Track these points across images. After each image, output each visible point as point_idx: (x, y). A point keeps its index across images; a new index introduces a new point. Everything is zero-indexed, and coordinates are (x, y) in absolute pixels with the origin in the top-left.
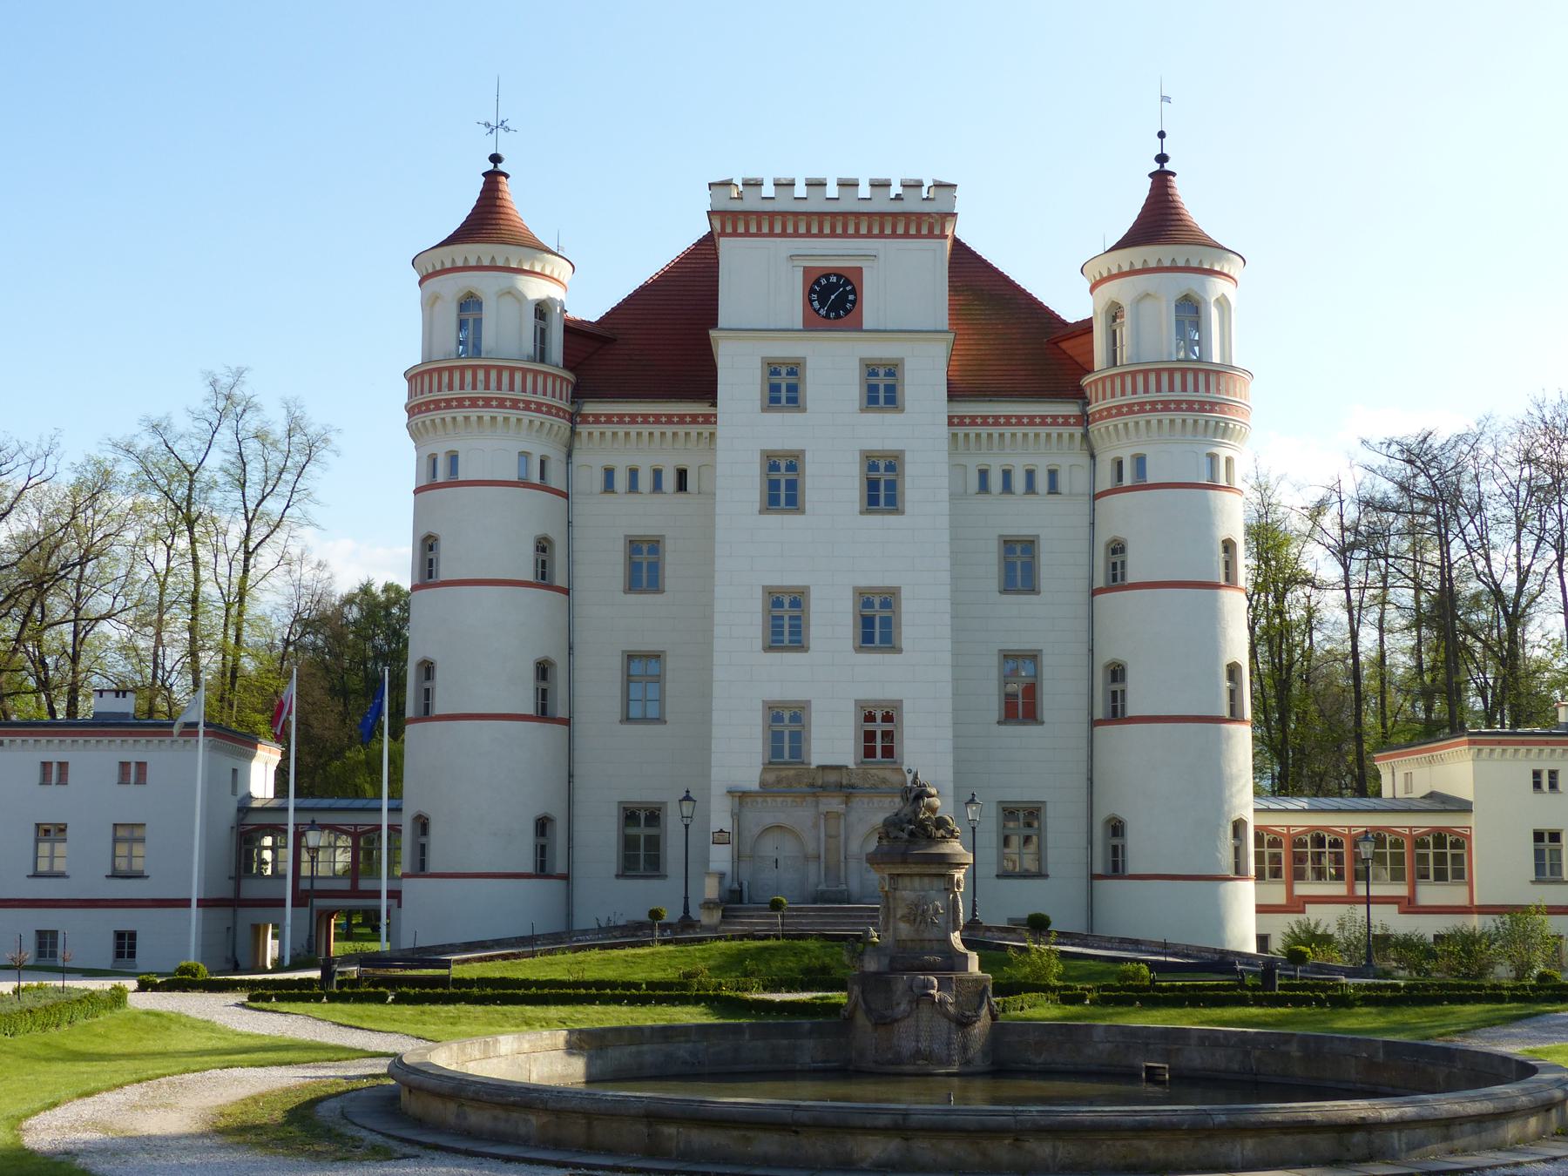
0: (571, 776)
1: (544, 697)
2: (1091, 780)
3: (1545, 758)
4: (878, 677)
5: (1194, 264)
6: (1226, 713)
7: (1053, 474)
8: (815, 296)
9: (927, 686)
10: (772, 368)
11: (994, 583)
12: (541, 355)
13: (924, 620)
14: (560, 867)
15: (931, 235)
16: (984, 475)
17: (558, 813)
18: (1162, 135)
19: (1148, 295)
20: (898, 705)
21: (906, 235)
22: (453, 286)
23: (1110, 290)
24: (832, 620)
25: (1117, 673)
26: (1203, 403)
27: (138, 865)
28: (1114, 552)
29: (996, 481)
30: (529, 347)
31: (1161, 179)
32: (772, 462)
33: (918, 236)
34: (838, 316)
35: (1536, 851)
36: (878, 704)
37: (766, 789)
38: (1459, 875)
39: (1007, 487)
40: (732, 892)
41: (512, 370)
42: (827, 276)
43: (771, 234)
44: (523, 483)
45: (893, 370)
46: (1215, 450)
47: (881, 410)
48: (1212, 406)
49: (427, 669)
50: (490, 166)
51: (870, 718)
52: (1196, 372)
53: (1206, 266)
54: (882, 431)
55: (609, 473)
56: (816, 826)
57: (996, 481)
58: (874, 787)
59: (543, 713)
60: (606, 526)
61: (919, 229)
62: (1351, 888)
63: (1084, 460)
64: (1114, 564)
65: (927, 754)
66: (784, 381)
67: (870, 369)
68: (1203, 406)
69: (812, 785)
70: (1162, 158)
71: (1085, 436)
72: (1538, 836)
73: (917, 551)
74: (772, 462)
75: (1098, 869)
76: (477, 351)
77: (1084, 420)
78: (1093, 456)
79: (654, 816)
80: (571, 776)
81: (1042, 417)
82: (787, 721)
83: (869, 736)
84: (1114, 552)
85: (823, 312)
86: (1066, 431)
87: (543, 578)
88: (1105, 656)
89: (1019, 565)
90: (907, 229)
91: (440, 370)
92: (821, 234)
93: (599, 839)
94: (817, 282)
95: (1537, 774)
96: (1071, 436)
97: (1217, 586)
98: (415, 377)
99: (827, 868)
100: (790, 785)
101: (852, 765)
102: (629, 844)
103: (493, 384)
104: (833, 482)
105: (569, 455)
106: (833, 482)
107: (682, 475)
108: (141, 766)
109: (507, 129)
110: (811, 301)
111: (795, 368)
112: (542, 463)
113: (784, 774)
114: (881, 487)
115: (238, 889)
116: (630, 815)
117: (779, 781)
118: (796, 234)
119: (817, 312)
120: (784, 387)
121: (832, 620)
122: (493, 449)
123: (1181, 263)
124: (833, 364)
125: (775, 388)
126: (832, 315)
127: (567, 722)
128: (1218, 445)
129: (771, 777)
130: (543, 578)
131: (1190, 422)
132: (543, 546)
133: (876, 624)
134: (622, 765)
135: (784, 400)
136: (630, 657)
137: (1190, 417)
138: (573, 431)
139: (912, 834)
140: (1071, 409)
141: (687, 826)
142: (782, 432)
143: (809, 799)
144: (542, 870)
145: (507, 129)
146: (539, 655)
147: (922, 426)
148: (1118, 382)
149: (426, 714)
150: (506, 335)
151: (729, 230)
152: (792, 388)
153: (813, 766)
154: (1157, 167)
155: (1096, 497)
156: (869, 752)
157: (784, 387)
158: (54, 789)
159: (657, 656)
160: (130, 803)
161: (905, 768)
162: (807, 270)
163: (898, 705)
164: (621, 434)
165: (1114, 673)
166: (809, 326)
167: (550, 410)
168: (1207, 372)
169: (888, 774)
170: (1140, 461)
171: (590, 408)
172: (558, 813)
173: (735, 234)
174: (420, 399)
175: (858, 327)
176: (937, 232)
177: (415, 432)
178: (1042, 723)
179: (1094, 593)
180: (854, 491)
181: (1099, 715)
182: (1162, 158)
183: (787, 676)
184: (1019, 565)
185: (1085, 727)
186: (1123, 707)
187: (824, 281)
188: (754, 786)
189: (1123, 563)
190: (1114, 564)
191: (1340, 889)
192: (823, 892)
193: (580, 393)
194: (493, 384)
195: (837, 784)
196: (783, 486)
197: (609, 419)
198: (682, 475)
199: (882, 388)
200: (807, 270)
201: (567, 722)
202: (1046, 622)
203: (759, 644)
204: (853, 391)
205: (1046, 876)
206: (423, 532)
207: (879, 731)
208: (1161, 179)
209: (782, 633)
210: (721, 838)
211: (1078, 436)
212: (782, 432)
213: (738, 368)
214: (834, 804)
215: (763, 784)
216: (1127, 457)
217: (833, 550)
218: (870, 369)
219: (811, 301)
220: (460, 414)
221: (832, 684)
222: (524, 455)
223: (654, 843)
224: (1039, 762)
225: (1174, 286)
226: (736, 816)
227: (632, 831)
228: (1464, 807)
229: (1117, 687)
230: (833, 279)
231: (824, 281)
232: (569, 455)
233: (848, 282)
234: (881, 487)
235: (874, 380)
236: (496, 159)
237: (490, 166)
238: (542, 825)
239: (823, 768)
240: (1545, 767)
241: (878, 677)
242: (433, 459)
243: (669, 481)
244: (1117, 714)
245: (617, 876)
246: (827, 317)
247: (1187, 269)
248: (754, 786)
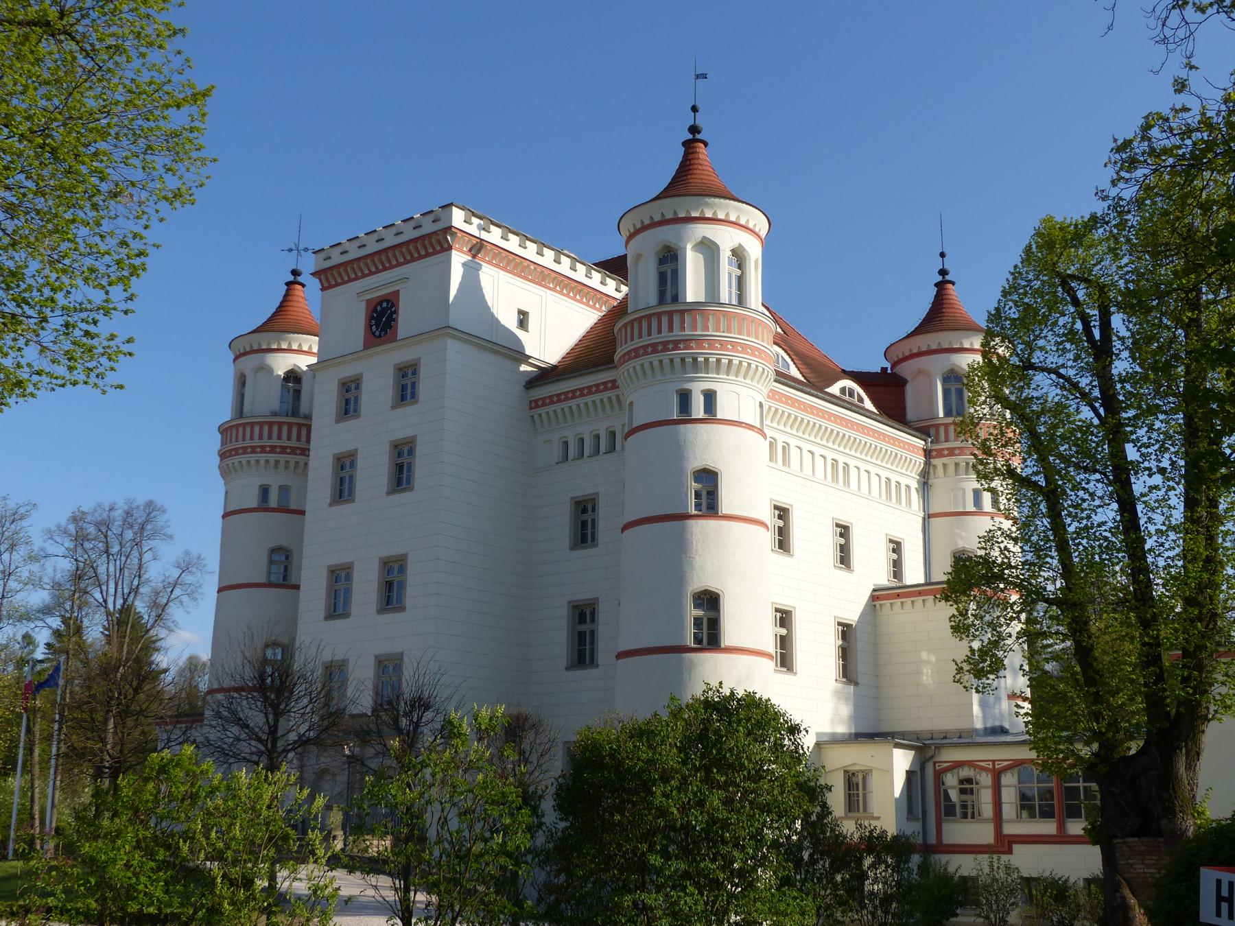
5: (669, 216)
6: (690, 642)
11: (566, 542)
18: (694, 109)
26: (665, 344)
42: (380, 303)
44: (263, 507)
46: (687, 386)
48: (687, 342)
52: (670, 314)
53: (682, 215)
54: (404, 422)
62: (1061, 826)
68: (665, 346)
70: (694, 129)
94: (375, 310)
97: (689, 517)
106: (373, 471)
110: (371, 326)
119: (374, 334)
123: (657, 218)
128: (692, 380)
131: (656, 363)
137: (655, 358)
162: (368, 302)
166: (367, 346)
168: (683, 312)
176: (446, 246)
182: (694, 129)
187: (379, 308)
191: (1048, 827)
199: (406, 388)
200: (368, 302)
219: (371, 326)
222: (265, 491)
230: (385, 305)
231: (379, 308)
236: (295, 273)
247: (665, 222)
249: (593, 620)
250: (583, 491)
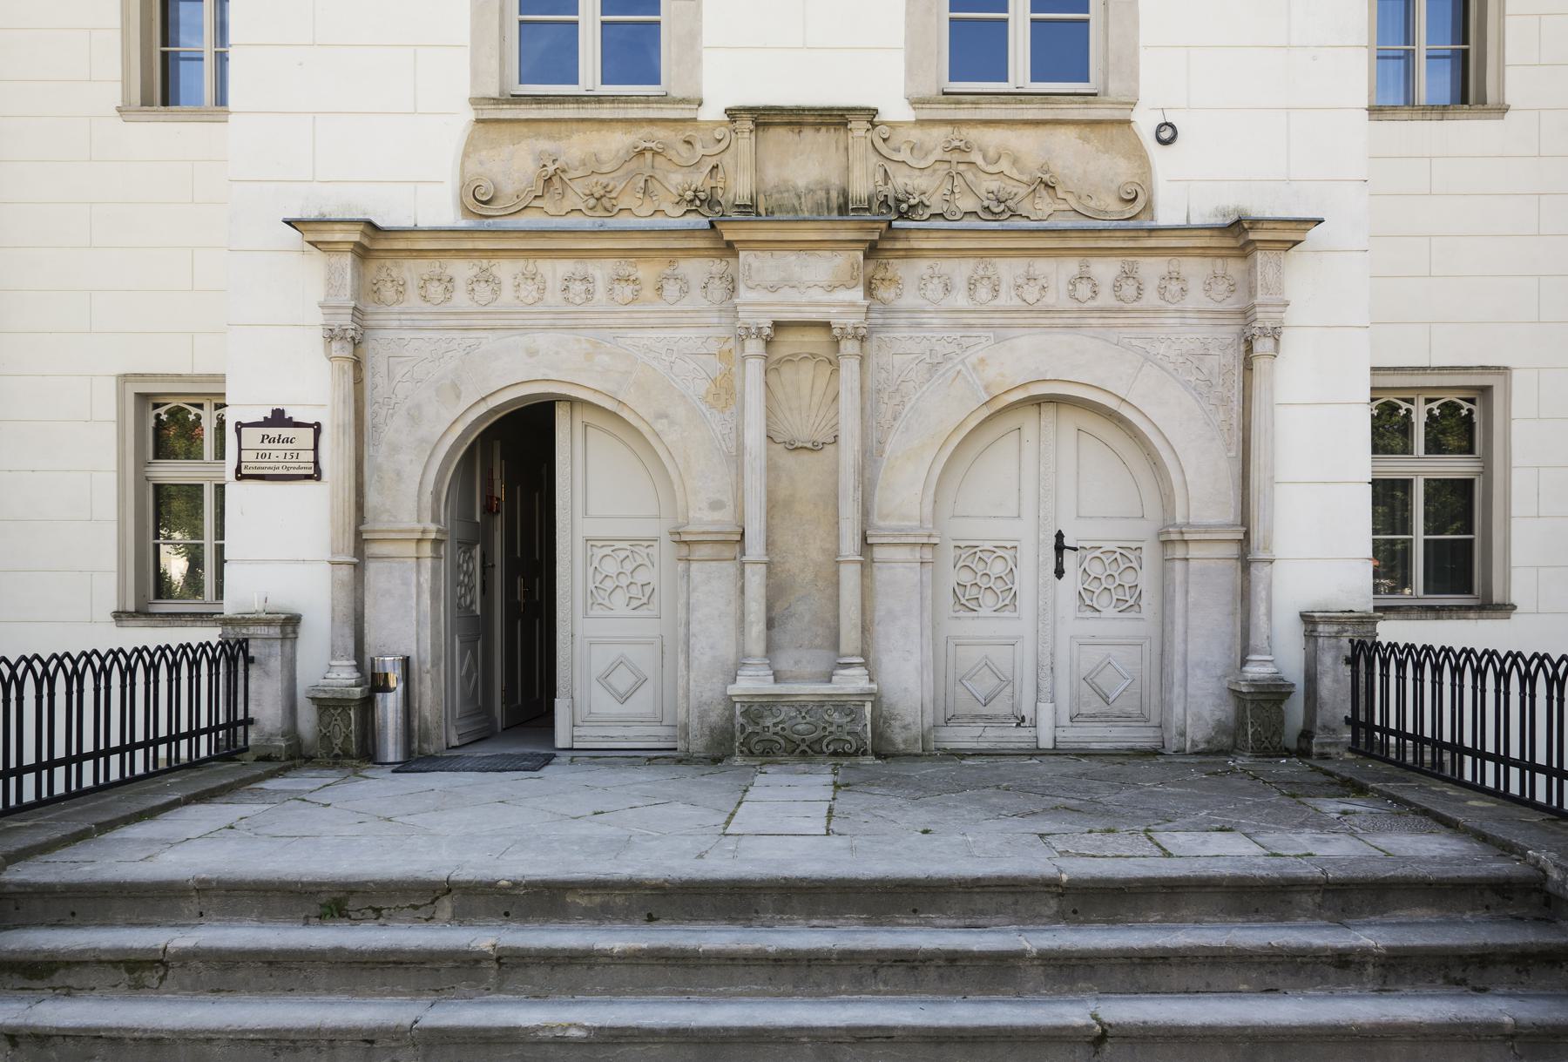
37: (488, 227)
40: (327, 705)
56: (726, 393)
58: (999, 209)
69: (702, 201)
99: (775, 592)
100: (602, 201)
101: (894, 109)
113: (575, 148)
117: (551, 180)
129: (514, 164)
143: (696, 269)
153: (712, 111)
161: (1145, 123)
169: (1067, 153)
178: (1502, 110)
188: (439, 208)
192: (756, 708)
214: (816, 282)
215: (478, 200)
226: (354, 345)
239: (764, 118)
248: (439, 208)
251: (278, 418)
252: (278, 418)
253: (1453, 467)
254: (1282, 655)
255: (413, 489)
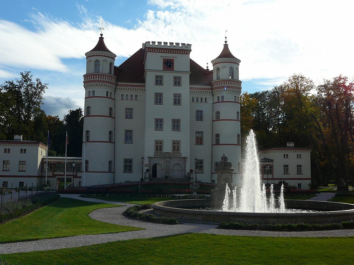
0: (115, 153)
1: (110, 138)
2: (212, 155)
3: (286, 152)
4: (177, 136)
7: (206, 99)
8: (165, 64)
9: (185, 137)
10: (157, 77)
12: (110, 73)
13: (185, 125)
14: (113, 171)
15: (187, 54)
16: (193, 98)
17: (113, 160)
18: (226, 38)
19: (224, 67)
20: (180, 141)
21: (182, 53)
22: (94, 59)
23: (218, 65)
24: (168, 125)
25: (218, 136)
27: (24, 169)
28: (217, 113)
29: (195, 100)
30: (108, 72)
31: (226, 46)
32: (157, 94)
33: (184, 54)
34: (169, 68)
35: (284, 169)
36: (176, 141)
38: (271, 173)
39: (197, 101)
41: (106, 76)
42: (167, 60)
43: (157, 52)
45: (179, 78)
47: (177, 86)
49: (88, 132)
50: (100, 36)
51: (174, 143)
54: (177, 90)
55: (122, 95)
57: (195, 100)
59: (110, 142)
60: (121, 106)
61: (185, 53)
63: (212, 97)
64: (217, 116)
65: (185, 150)
66: (159, 79)
67: (175, 78)
70: (226, 42)
71: (212, 92)
72: (284, 166)
73: (184, 113)
74: (157, 94)
75: (213, 171)
76: (99, 72)
77: (212, 89)
78: (213, 96)
79: (130, 161)
80: (115, 153)
81: (206, 88)
82: (159, 144)
83: (174, 147)
84: (217, 113)
85: (166, 67)
86: (208, 91)
87: (110, 116)
88: (215, 132)
89: (199, 116)
90: (182, 52)
91: (91, 75)
92: (166, 53)
93: (120, 165)
94: (166, 61)
95: (284, 155)
96: (209, 92)
98: (84, 76)
99: (166, 171)
101: (171, 152)
102: (126, 166)
103: (102, 78)
104: (168, 99)
105: (115, 92)
106: (168, 99)
107: (136, 96)
108: (25, 150)
109: (104, 29)
111: (161, 77)
112: (111, 93)
114: (177, 101)
115: (42, 174)
116: (126, 161)
118: (162, 52)
120: (159, 81)
121: (168, 125)
122: (101, 91)
124: (168, 77)
125: (157, 81)
126: (168, 68)
127: (114, 143)
130: (110, 116)
132: (111, 109)
133: (176, 125)
134: (124, 151)
135: (159, 84)
136: (126, 131)
138: (116, 88)
139: (224, 165)
140: (210, 87)
141: (143, 163)
142: (159, 89)
144: (110, 171)
145: (104, 29)
146: (110, 130)
147: (185, 89)
148: (217, 83)
149: (88, 141)
150: (105, 69)
151: (149, 51)
152: (161, 81)
154: (225, 43)
155: (214, 103)
156: (174, 150)
157: (159, 81)
158: (7, 154)
159: (131, 131)
160: (23, 157)
163: (180, 141)
164: (125, 88)
165: (217, 136)
166: (164, 69)
167: (112, 83)
170: (223, 97)
171: (119, 83)
172: (113, 160)
173: (150, 52)
174: (87, 80)
175: (173, 70)
176: (188, 53)
177: (85, 87)
178: (203, 145)
179: (213, 121)
180: (172, 101)
181: (214, 143)
182: (226, 42)
183: (159, 135)
184: (199, 116)
185: (211, 146)
186: (219, 142)
189: (219, 116)
190: (217, 116)
193: (118, 80)
194: (102, 78)
195: (168, 156)
196: (159, 99)
197: (123, 85)
198: (136, 96)
199: (177, 82)
201: (114, 143)
202: (205, 126)
203: (154, 129)
204: (172, 82)
205: (204, 173)
206: (87, 106)
207: (176, 145)
208: (226, 46)
209: (158, 127)
210: (146, 165)
211: (211, 92)
212: (159, 89)
213: (150, 78)
214: (168, 159)
215: (154, 156)
216: (220, 96)
217: (168, 111)
218: (175, 78)
220: (96, 83)
221: (167, 136)
222: (107, 93)
223: (130, 166)
224: (203, 152)
225: (229, 65)
226: (149, 161)
227: (126, 164)
228: (272, 161)
229: (218, 138)
230: (169, 61)
231: (167, 61)
232: (115, 92)
233: (171, 62)
234: (177, 101)
235: (176, 80)
236: (102, 35)
237: (100, 36)
238: (110, 162)
239: (166, 153)
240: (286, 154)
241: (177, 136)
242: (89, 91)
243: (134, 97)
244: (218, 143)
245: (123, 172)
246: (167, 68)
249: (219, 137)
250: (200, 109)
251: (146, 164)
252: (146, 164)
253: (201, 165)
254: (186, 174)
255: (151, 168)
